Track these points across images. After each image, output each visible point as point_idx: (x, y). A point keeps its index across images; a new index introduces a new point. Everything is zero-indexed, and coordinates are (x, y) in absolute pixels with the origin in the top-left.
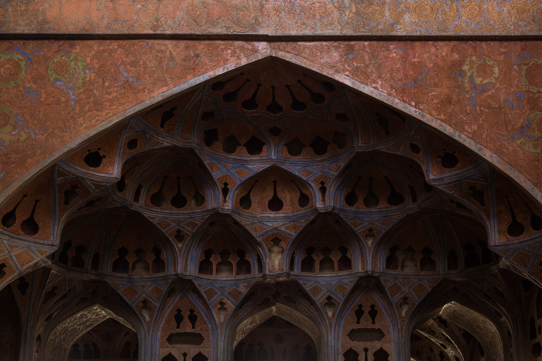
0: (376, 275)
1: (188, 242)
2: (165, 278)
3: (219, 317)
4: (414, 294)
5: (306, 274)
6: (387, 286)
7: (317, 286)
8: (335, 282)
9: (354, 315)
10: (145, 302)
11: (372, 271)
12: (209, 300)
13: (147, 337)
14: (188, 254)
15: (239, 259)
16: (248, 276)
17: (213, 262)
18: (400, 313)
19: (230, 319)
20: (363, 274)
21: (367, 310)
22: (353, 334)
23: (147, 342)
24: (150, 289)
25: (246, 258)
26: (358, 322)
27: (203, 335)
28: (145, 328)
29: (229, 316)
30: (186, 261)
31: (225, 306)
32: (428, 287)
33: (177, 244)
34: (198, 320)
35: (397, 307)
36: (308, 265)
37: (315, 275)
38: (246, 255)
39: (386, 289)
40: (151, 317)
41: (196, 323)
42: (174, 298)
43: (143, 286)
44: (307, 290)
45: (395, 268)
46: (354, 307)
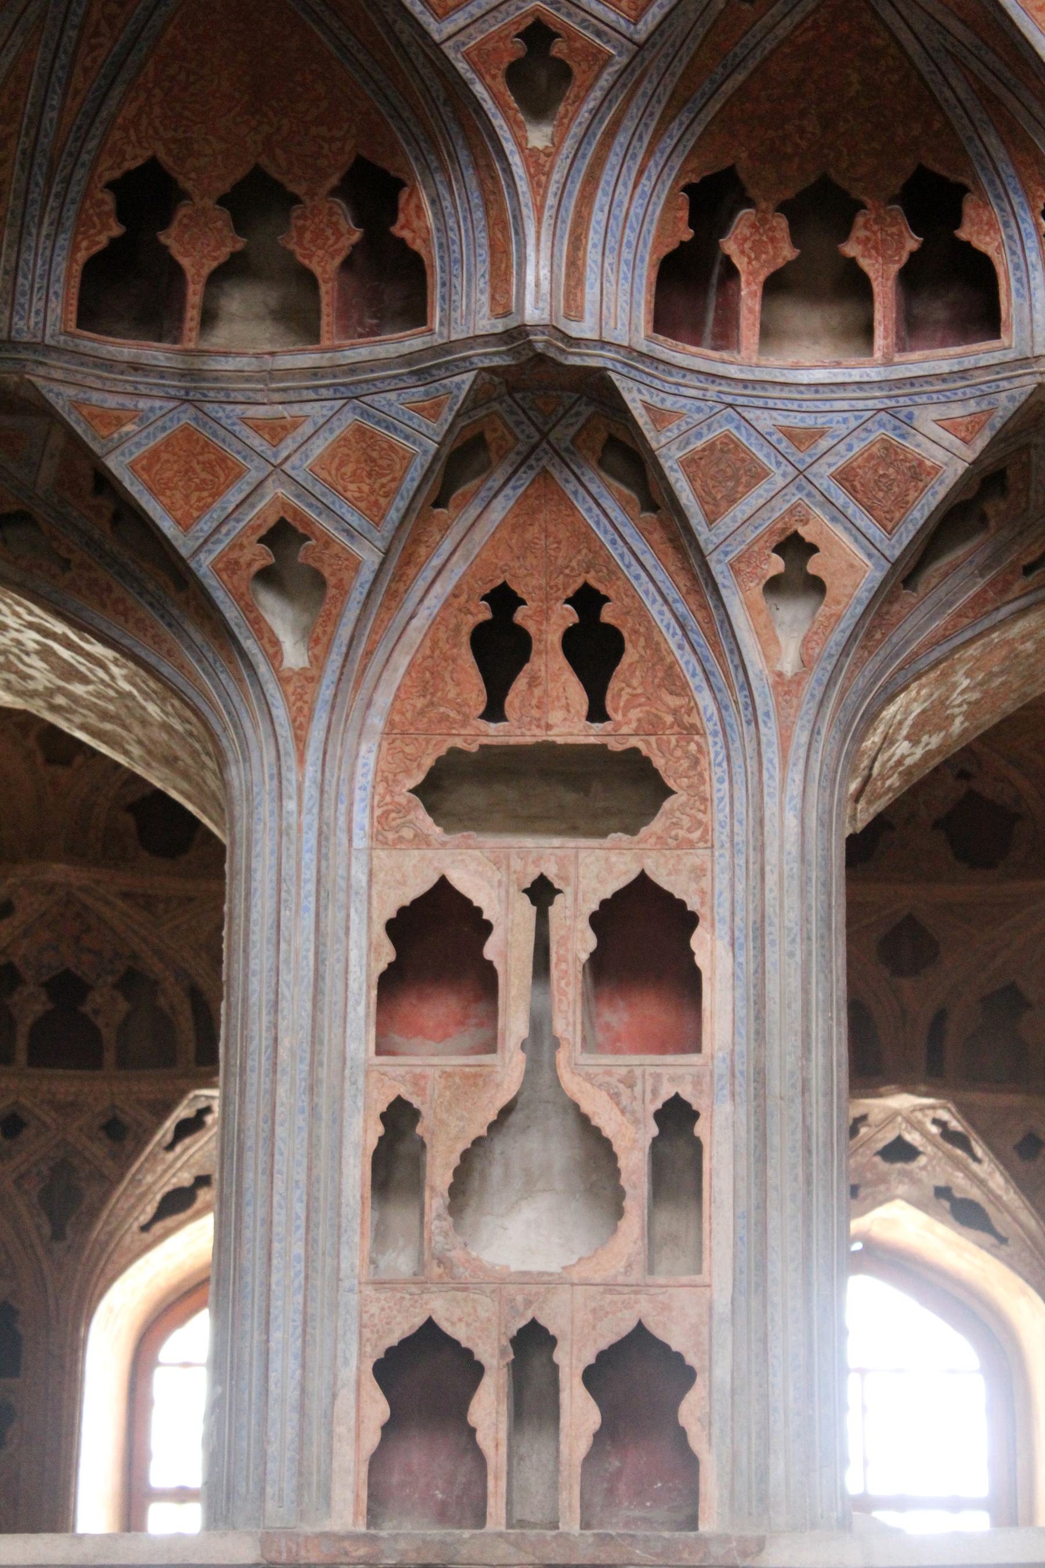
1: (595, 113)
2: (423, 369)
3: (768, 642)
10: (282, 535)
12: (711, 519)
13: (291, 776)
14: (586, 198)
15: (912, 243)
16: (981, 353)
17: (740, 263)
19: (845, 652)
23: (291, 805)
24: (319, 447)
25: (963, 234)
28: (280, 712)
29: (838, 636)
30: (577, 242)
31: (814, 565)
33: (514, 124)
34: (630, 655)
38: (969, 210)
40: (316, 640)
42: (473, 512)
43: (276, 431)
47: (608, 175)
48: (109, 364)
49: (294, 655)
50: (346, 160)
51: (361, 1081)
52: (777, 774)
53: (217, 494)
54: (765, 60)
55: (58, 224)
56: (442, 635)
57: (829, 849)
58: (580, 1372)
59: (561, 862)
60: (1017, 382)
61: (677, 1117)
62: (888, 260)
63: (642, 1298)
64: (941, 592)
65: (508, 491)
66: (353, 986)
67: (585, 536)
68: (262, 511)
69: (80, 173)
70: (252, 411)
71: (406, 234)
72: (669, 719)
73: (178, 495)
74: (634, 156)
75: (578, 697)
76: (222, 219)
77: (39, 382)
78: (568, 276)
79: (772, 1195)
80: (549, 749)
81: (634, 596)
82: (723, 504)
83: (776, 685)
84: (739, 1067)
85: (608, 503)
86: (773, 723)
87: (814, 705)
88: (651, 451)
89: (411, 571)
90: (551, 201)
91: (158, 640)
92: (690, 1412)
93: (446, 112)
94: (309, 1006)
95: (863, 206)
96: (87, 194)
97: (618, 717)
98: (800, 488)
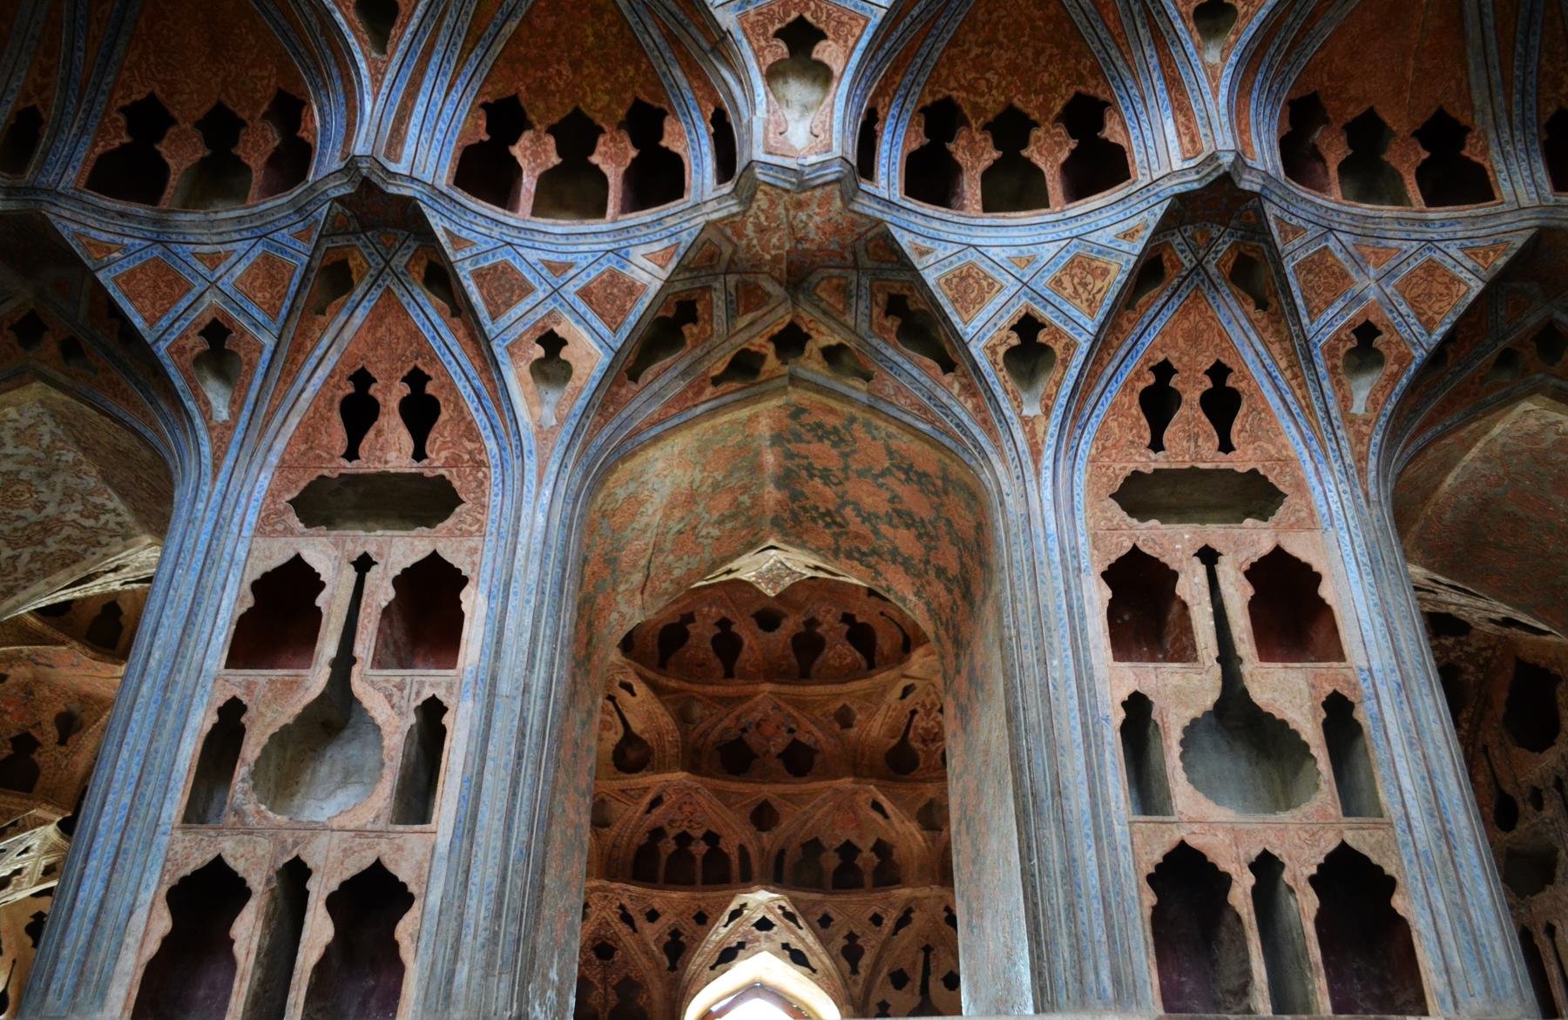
0: (1249, 183)
4: (1404, 309)
5: (928, 209)
6: (1294, 253)
7: (972, 265)
8: (1053, 249)
9: (1136, 410)
10: (217, 332)
11: (1239, 156)
12: (494, 317)
16: (673, 207)
18: (1346, 401)
20: (1192, 183)
21: (1192, 389)
22: (1138, 496)
23: (200, 506)
24: (239, 270)
25: (664, 143)
26: (1156, 445)
27: (456, 484)
28: (206, 449)
29: (581, 403)
32: (1465, 275)
34: (444, 415)
35: (1333, 370)
36: (931, 179)
37: (962, 220)
38: (668, 125)
39: (1289, 267)
40: (236, 404)
41: (432, 435)
42: (342, 318)
43: (214, 260)
44: (931, 277)
45: (1322, 189)
46: (1138, 375)
47: (427, 84)
48: (104, 212)
49: (222, 412)
50: (271, 92)
51: (210, 685)
52: (534, 490)
53: (174, 302)
54: (529, 12)
55: (83, 130)
56: (322, 404)
57: (568, 541)
58: (324, 896)
59: (380, 547)
60: (693, 223)
61: (432, 712)
62: (618, 165)
63: (383, 841)
64: (656, 386)
65: (365, 303)
66: (220, 622)
67: (415, 334)
68: (203, 312)
69: (102, 98)
70: (200, 249)
71: (305, 135)
72: (466, 457)
73: (147, 302)
74: (445, 74)
75: (406, 441)
76: (197, 138)
77: (51, 217)
78: (391, 136)
79: (490, 764)
80: (385, 476)
81: (448, 375)
82: (502, 308)
83: (537, 433)
84: (481, 676)
85: (430, 311)
86: (534, 458)
87: (562, 449)
88: (451, 264)
89: (301, 358)
90: (384, 90)
91: (145, 415)
92: (405, 929)
93: (322, 40)
94: (179, 632)
95: (602, 131)
96: (106, 113)
97: (433, 456)
98: (555, 300)
